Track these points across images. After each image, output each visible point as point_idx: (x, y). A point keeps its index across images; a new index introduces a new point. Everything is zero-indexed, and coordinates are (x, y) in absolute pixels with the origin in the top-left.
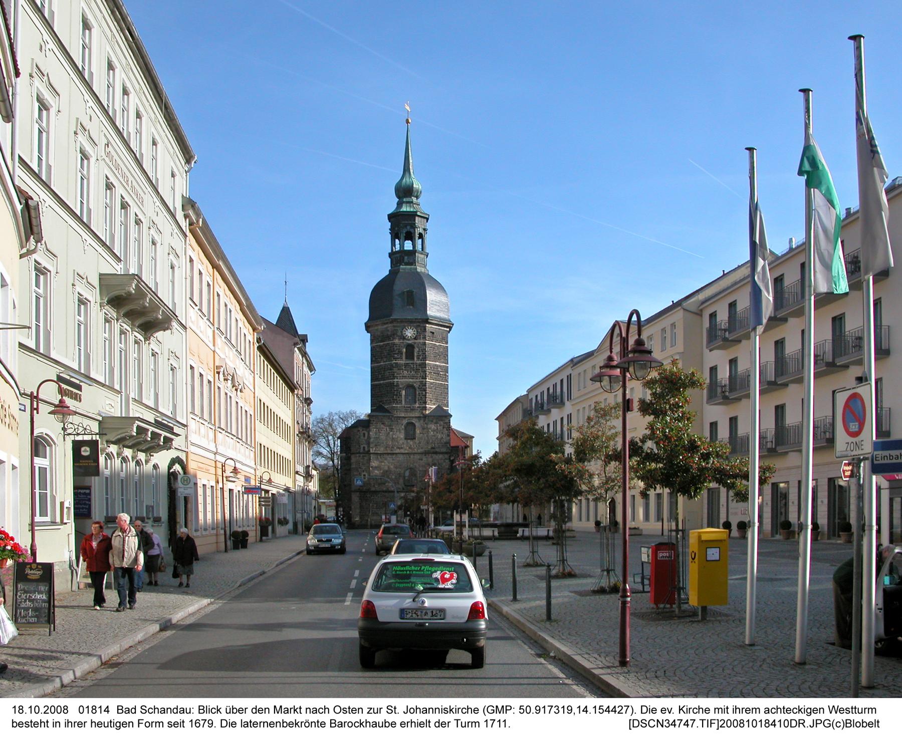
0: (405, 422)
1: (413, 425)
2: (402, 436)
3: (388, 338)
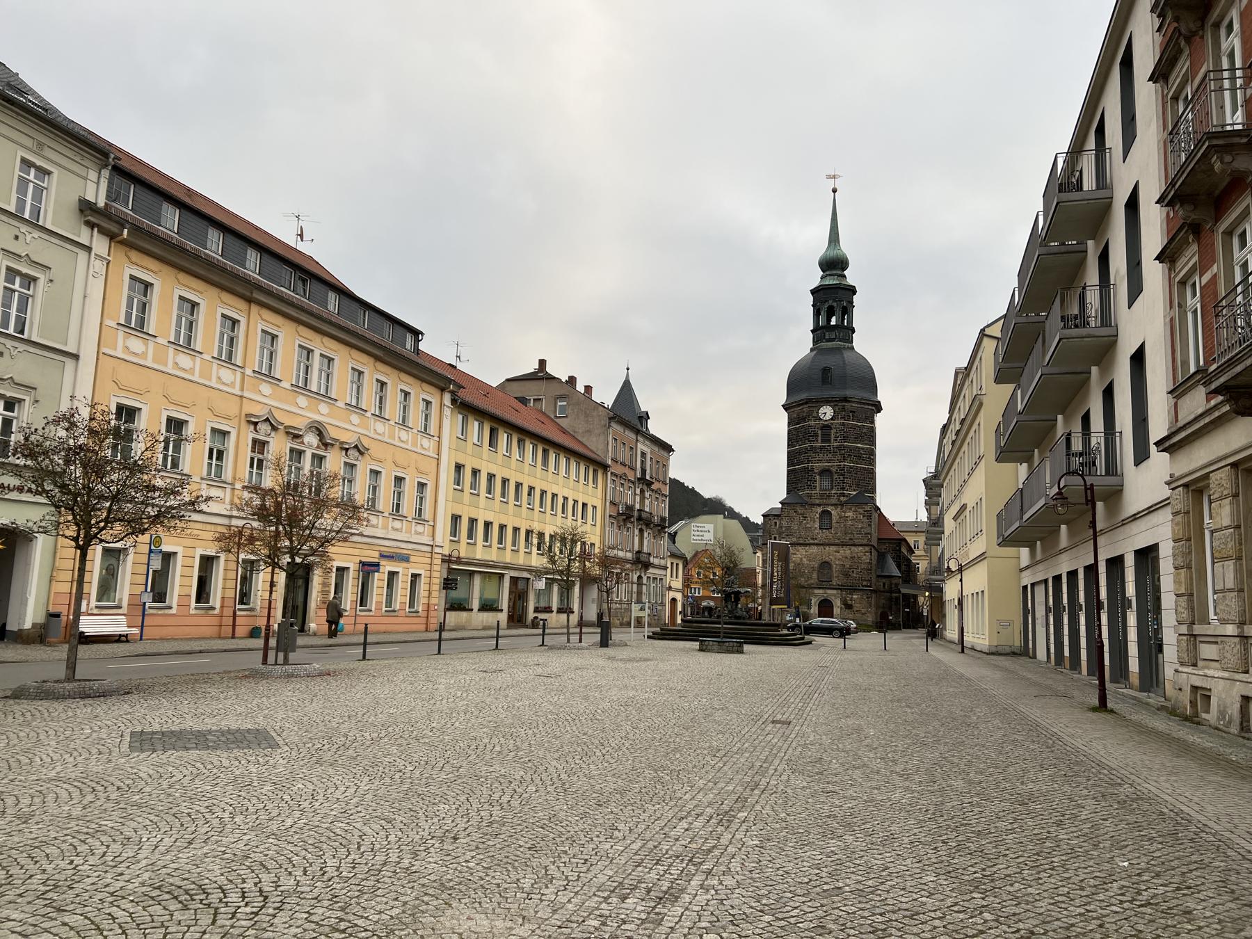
0: (820, 510)
1: (829, 513)
2: (817, 525)
3: (804, 419)
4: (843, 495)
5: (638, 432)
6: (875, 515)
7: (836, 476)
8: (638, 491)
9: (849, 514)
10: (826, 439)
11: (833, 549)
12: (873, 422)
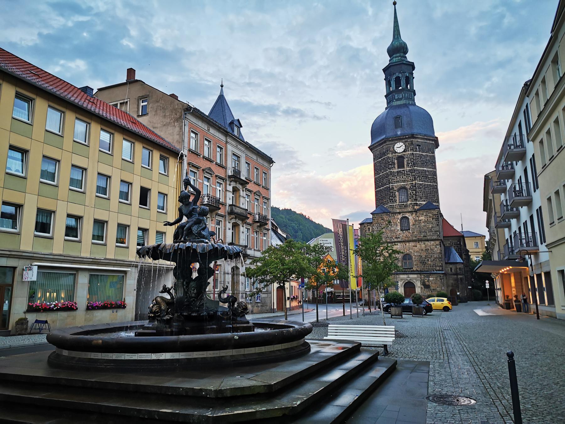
0: (400, 216)
1: (408, 219)
2: (399, 228)
3: (384, 154)
4: (416, 204)
5: (226, 134)
6: (440, 220)
7: (410, 191)
8: (230, 188)
9: (422, 218)
10: (401, 165)
11: (412, 244)
12: (434, 153)
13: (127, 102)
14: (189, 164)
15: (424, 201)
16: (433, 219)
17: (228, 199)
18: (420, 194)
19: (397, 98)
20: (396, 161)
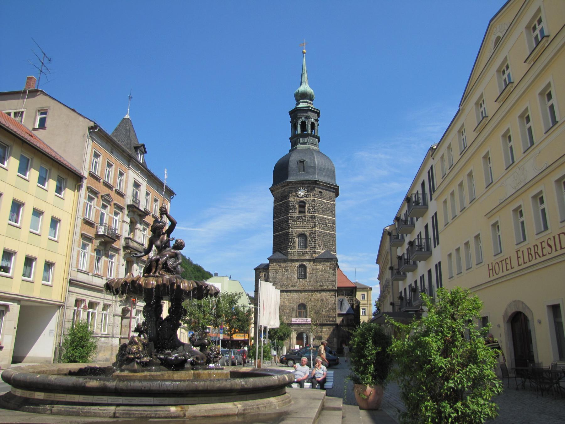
0: (298, 264)
10: (302, 210)
13: (22, 112)
14: (88, 188)
15: (323, 249)
16: (330, 268)
17: (124, 231)
18: (319, 242)
19: (301, 142)
20: (297, 206)
